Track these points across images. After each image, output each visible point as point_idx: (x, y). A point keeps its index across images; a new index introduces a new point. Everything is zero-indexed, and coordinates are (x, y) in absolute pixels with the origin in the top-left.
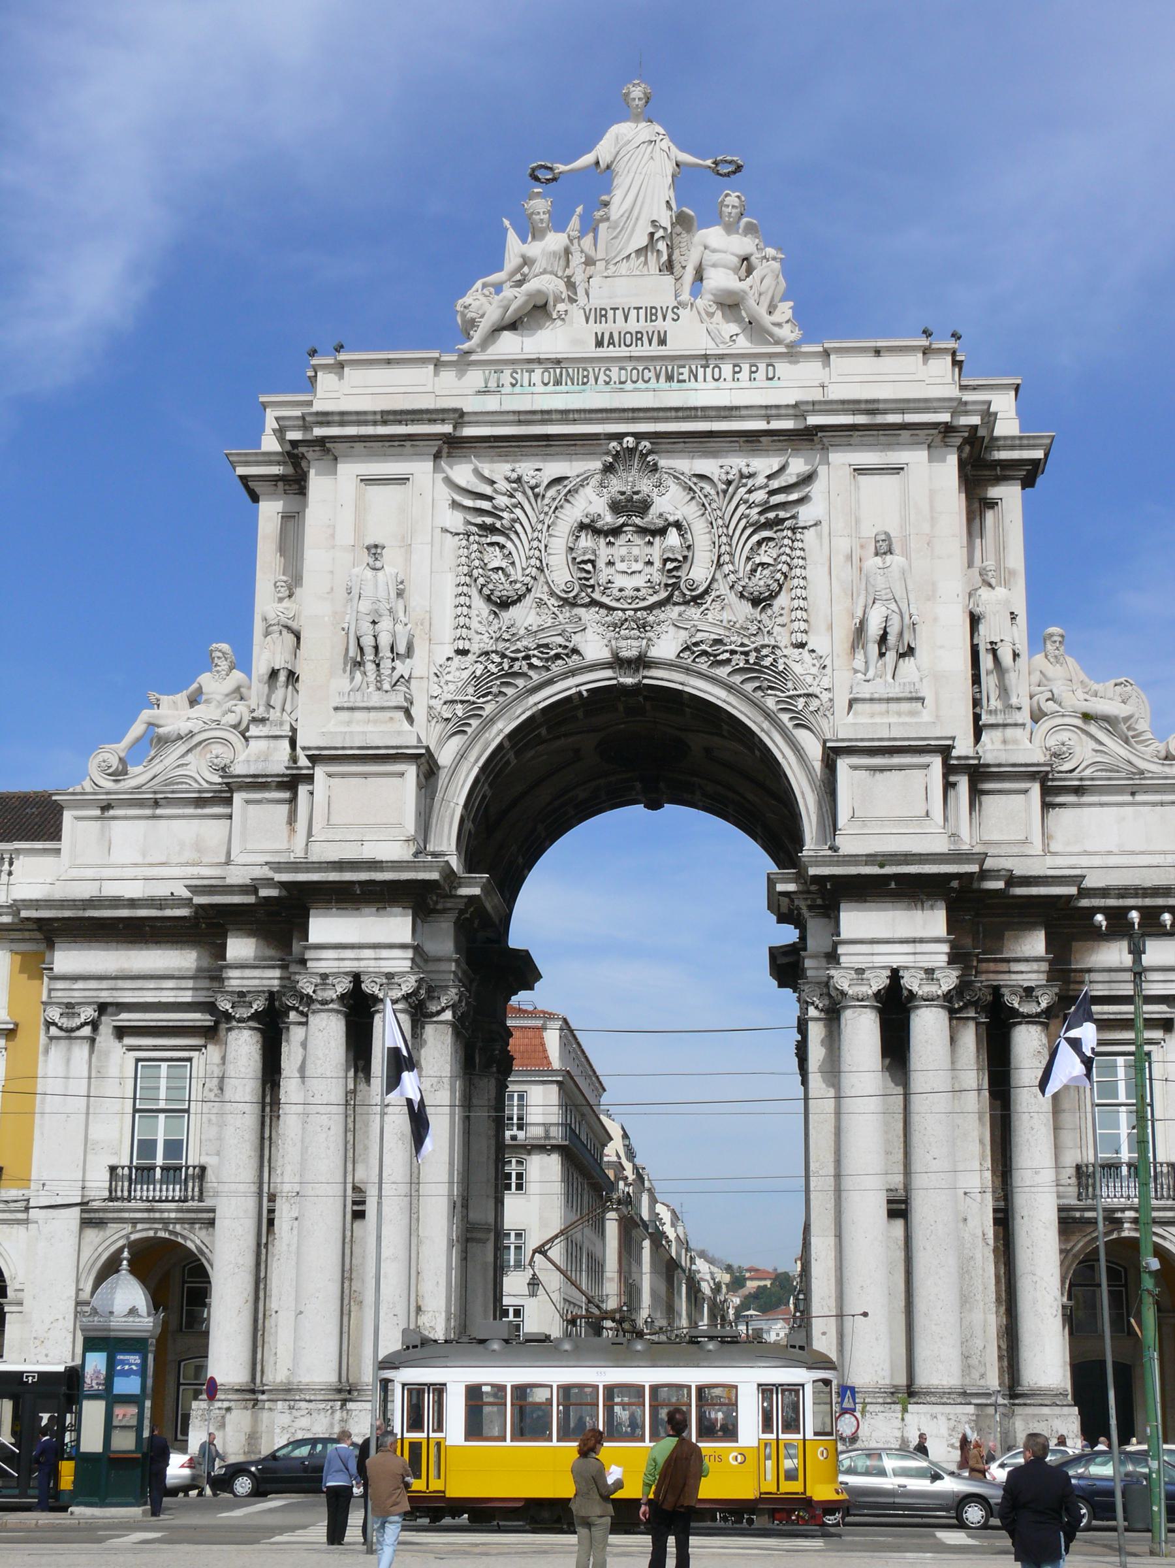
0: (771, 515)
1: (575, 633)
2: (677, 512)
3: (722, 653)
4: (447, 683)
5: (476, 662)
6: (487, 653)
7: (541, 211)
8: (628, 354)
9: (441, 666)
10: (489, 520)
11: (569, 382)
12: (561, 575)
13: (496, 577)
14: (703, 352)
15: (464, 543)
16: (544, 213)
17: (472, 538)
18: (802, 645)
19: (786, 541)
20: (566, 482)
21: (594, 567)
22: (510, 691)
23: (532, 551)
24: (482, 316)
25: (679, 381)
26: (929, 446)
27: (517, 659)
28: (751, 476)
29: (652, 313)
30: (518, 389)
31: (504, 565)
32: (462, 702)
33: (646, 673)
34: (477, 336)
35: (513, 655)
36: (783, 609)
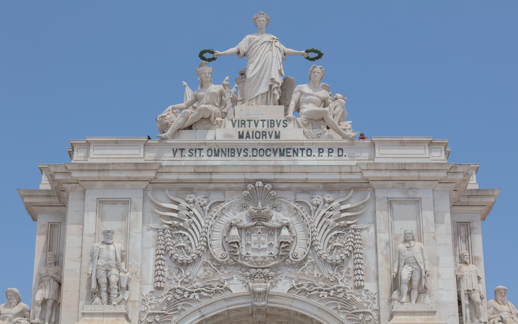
0: (343, 222)
1: (225, 279)
2: (288, 218)
3: (315, 290)
4: (150, 304)
5: (168, 294)
6: (175, 289)
7: (207, 72)
8: (258, 142)
9: (146, 295)
10: (176, 222)
11: (223, 156)
12: (218, 251)
13: (180, 251)
14: (302, 142)
15: (161, 233)
16: (208, 73)
17: (166, 231)
18: (360, 287)
19: (351, 235)
20: (221, 204)
21: (239, 246)
22: (188, 310)
23: (202, 238)
24: (172, 122)
25: (287, 156)
26: (433, 190)
27: (193, 292)
28: (330, 203)
29: (272, 123)
30: (193, 158)
31: (185, 245)
32: (159, 314)
33: (270, 300)
34: (169, 132)
35: (189, 290)
36: (349, 269)
